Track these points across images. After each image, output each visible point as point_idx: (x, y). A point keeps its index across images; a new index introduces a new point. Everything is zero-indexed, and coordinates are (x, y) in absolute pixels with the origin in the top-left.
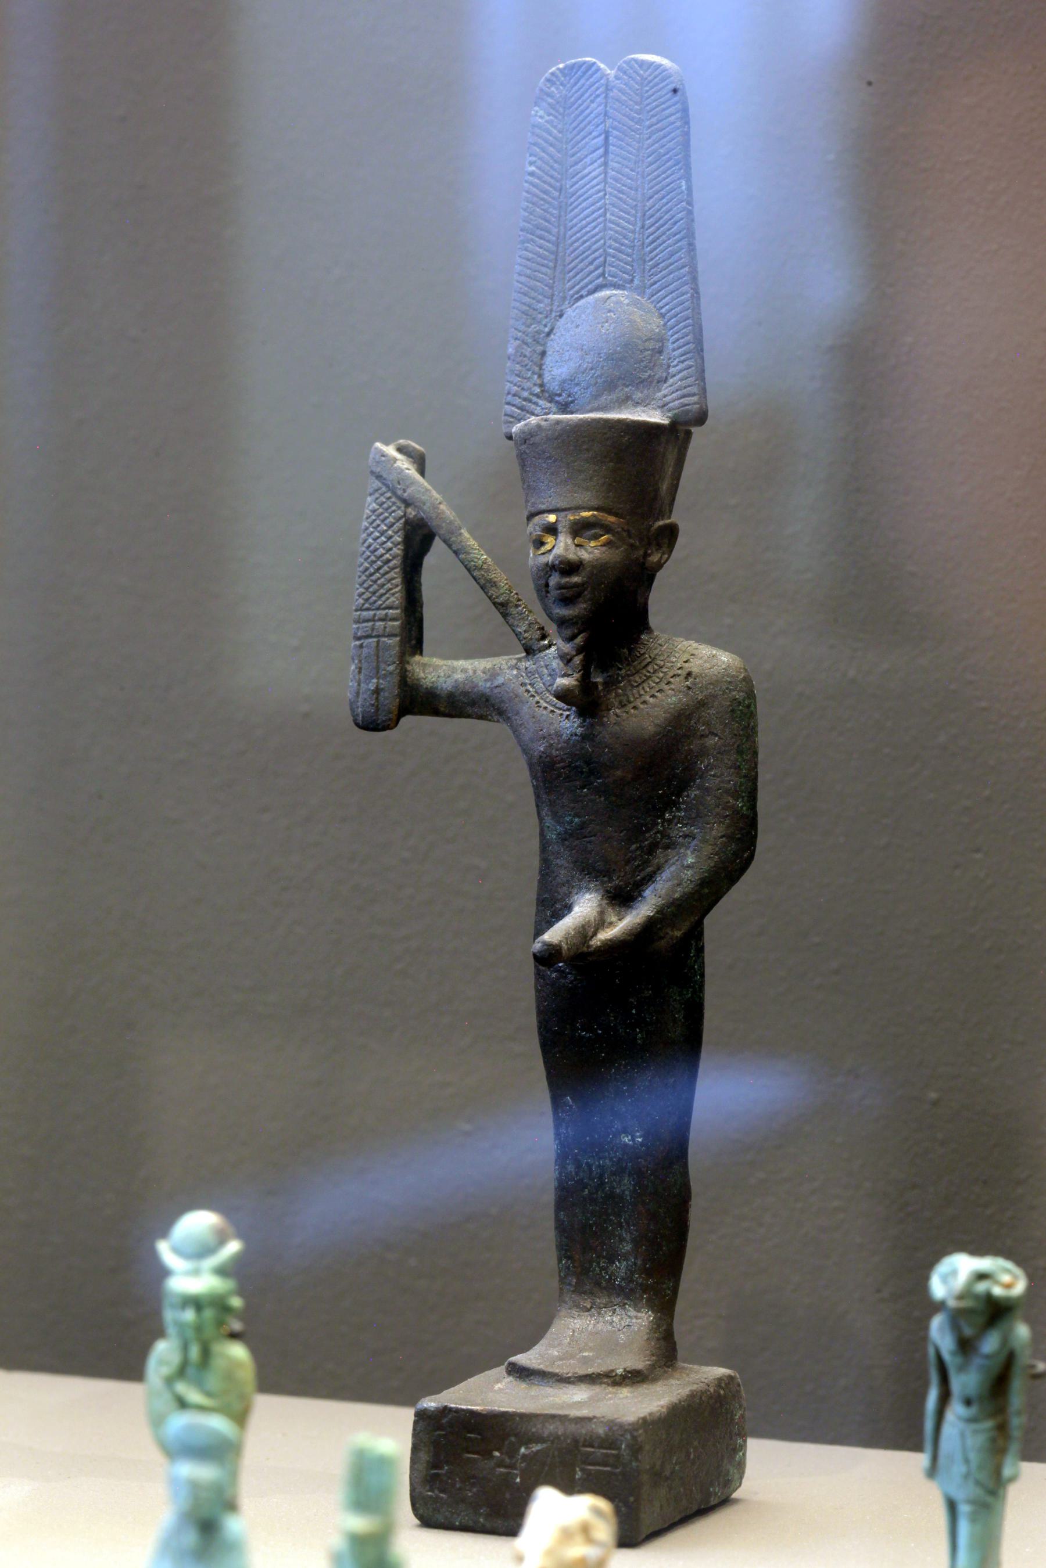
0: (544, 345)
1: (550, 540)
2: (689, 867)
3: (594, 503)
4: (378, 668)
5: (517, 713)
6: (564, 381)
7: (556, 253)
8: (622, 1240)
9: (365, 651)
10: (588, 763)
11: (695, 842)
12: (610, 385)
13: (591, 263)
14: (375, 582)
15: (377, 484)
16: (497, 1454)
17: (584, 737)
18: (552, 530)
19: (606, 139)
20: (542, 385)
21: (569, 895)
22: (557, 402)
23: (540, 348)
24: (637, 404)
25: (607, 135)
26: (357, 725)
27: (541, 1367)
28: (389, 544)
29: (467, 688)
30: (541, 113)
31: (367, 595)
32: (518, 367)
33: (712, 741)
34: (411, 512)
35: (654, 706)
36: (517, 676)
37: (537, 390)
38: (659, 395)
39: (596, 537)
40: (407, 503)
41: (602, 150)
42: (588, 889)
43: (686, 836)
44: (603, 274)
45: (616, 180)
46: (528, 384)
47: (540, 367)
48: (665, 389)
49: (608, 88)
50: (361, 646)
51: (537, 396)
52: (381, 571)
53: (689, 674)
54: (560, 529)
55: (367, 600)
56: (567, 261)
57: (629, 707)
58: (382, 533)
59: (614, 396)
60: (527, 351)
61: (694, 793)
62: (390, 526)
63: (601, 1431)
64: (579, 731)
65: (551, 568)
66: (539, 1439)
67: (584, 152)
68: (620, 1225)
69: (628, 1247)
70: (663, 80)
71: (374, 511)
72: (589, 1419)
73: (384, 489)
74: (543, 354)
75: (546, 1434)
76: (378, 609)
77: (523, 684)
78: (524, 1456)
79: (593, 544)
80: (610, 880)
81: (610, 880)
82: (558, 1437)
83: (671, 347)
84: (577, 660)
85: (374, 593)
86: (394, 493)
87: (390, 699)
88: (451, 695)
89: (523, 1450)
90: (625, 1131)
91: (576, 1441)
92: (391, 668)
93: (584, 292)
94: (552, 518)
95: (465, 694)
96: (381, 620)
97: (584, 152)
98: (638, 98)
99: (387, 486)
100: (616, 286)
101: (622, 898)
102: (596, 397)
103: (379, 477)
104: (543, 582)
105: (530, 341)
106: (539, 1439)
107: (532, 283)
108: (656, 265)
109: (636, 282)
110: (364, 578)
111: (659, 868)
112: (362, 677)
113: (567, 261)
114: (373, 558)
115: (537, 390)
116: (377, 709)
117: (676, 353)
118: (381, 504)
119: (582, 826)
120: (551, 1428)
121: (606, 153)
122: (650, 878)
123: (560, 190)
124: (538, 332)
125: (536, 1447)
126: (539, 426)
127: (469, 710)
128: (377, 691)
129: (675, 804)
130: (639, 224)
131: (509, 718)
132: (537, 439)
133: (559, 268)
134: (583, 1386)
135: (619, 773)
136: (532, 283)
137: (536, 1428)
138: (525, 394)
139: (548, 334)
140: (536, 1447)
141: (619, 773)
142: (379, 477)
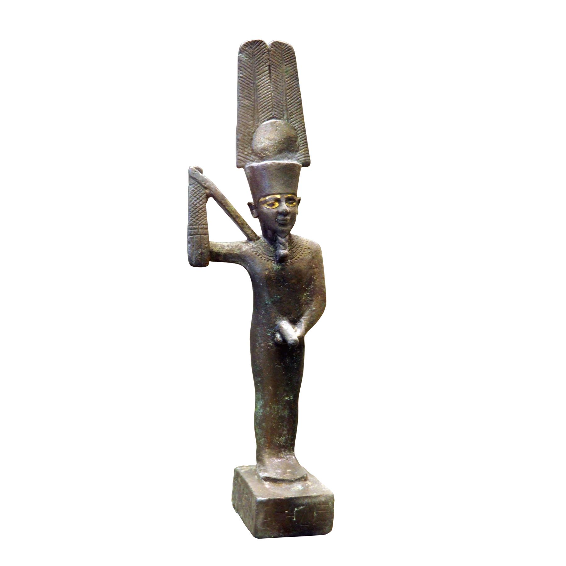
0: (252, 136)
1: (277, 204)
2: (314, 311)
3: (292, 192)
4: (201, 245)
5: (253, 261)
6: (262, 149)
7: (254, 105)
8: (283, 430)
9: (195, 239)
10: (283, 278)
11: (313, 303)
12: (280, 151)
13: (268, 110)
14: (197, 215)
15: (193, 181)
16: (287, 512)
17: (282, 269)
18: (278, 200)
19: (269, 68)
20: (252, 150)
21: (275, 322)
22: (259, 156)
23: (250, 138)
24: (289, 158)
25: (269, 66)
26: (192, 265)
27: (281, 478)
28: (201, 203)
29: (232, 252)
30: (243, 56)
31: (194, 220)
32: (242, 143)
33: (316, 270)
34: (207, 191)
35: (302, 259)
36: (250, 249)
37: (250, 152)
38: (296, 156)
39: (292, 203)
40: (206, 188)
41: (268, 72)
42: (283, 319)
43: (311, 301)
44: (272, 114)
45: (275, 83)
46: (246, 150)
47: (251, 144)
48: (298, 154)
49: (269, 51)
50: (193, 238)
51: (251, 154)
52: (200, 212)
53: (309, 248)
54: (282, 200)
55: (194, 222)
56: (259, 108)
57: (294, 259)
58: (198, 199)
59: (281, 155)
60: (246, 138)
61: (312, 287)
62: (200, 197)
63: (323, 499)
64: (280, 267)
65: (279, 213)
66: (302, 505)
67: (261, 72)
68: (283, 426)
69: (285, 432)
70: (289, 50)
71: (193, 191)
72: (319, 496)
73: (196, 183)
74: (252, 139)
75: (304, 503)
76: (199, 225)
77: (253, 251)
78: (297, 511)
79: (291, 205)
80: (291, 316)
81: (291, 316)
82: (308, 503)
83: (299, 140)
84: (287, 244)
85: (197, 219)
86: (201, 185)
87: (206, 256)
88: (225, 255)
89: (296, 509)
90: (287, 396)
91: (315, 504)
92: (207, 246)
93: (265, 119)
94: (278, 196)
95: (231, 254)
96: (201, 229)
97: (261, 72)
98: (280, 55)
99: (199, 183)
100: (277, 118)
101: (294, 322)
102: (276, 155)
103: (194, 179)
104: (274, 218)
105: (246, 134)
106: (302, 505)
107: (246, 115)
108: (292, 112)
109: (285, 117)
110: (192, 214)
111: (304, 312)
112: (194, 248)
113: (259, 108)
114: (195, 207)
115: (250, 152)
116: (201, 260)
117: (302, 142)
118: (196, 189)
119: (281, 299)
120: (306, 500)
121: (270, 73)
122: (302, 315)
123: (254, 84)
124: (250, 132)
125: (301, 508)
126: (271, 165)
127: (230, 260)
128: (202, 253)
129: (307, 290)
130: (285, 98)
131: (249, 263)
132: (270, 169)
133: (256, 111)
134: (297, 482)
135: (293, 281)
136: (246, 115)
137: (301, 502)
138: (246, 153)
139: (253, 133)
140: (301, 508)
141: (293, 281)
142: (194, 179)
